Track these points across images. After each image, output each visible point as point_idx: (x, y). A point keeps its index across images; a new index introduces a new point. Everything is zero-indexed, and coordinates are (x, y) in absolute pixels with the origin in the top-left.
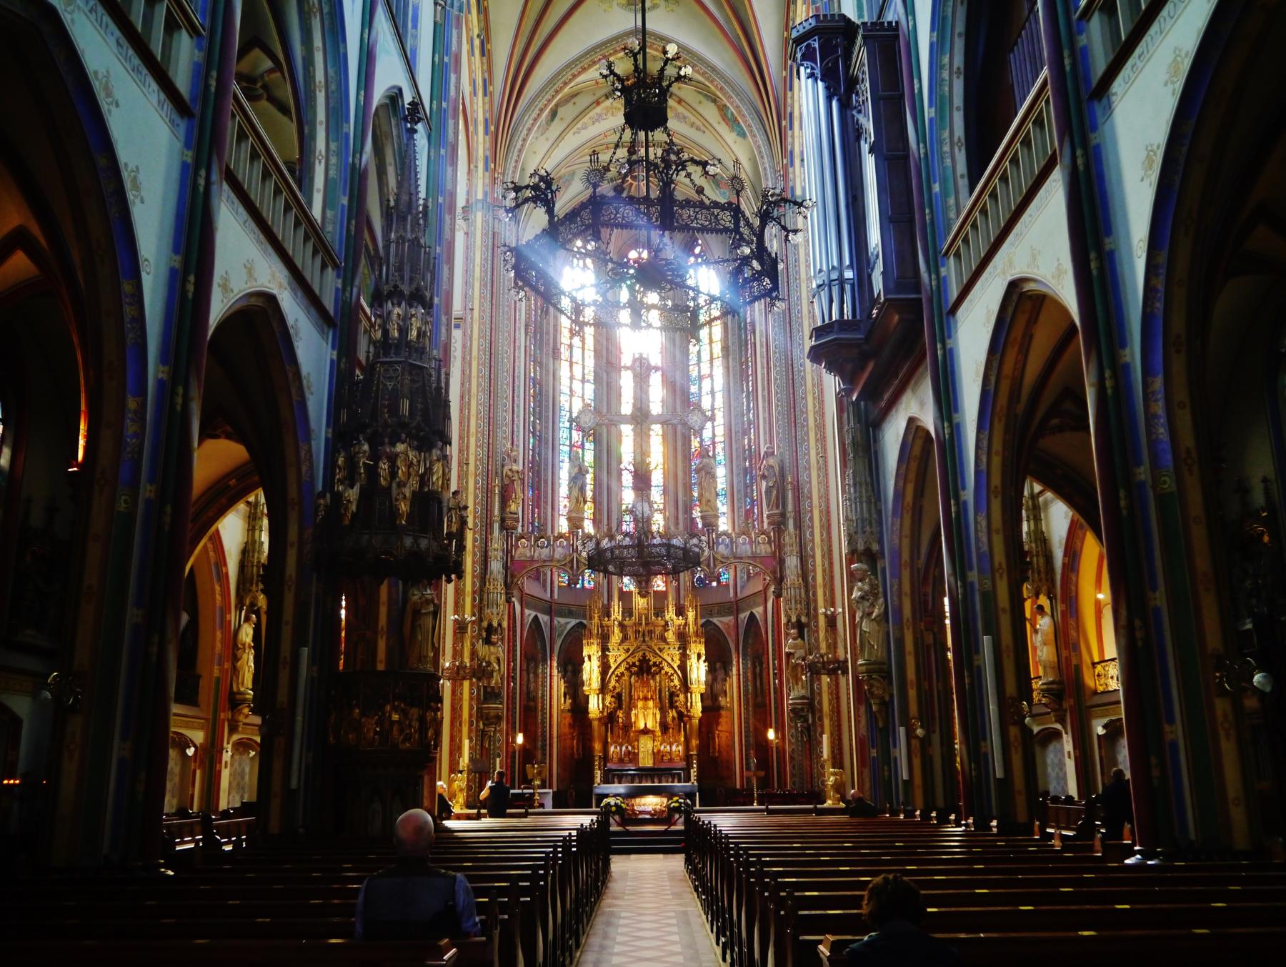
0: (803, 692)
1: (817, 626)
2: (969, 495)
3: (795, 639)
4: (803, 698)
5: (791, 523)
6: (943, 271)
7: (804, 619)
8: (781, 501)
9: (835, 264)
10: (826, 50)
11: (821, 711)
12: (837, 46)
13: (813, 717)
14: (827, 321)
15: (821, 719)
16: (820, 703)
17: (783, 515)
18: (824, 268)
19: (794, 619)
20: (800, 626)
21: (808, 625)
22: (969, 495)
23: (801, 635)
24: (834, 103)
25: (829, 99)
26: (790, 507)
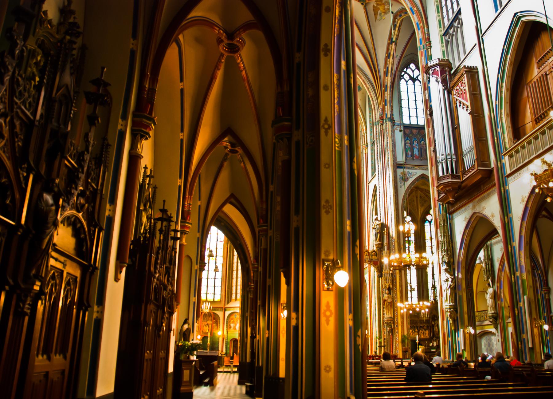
0: (390, 316)
1: (396, 289)
2: (516, 244)
3: (388, 294)
4: (391, 318)
5: (385, 248)
6: (503, 161)
7: (391, 286)
8: (381, 239)
9: (449, 152)
10: (443, 72)
11: (397, 323)
12: (446, 71)
13: (394, 325)
14: (445, 174)
15: (397, 326)
16: (397, 320)
17: (382, 244)
18: (444, 154)
19: (387, 287)
20: (389, 289)
21: (392, 289)
22: (516, 244)
23: (389, 293)
24: (446, 92)
25: (444, 90)
26: (385, 242)
